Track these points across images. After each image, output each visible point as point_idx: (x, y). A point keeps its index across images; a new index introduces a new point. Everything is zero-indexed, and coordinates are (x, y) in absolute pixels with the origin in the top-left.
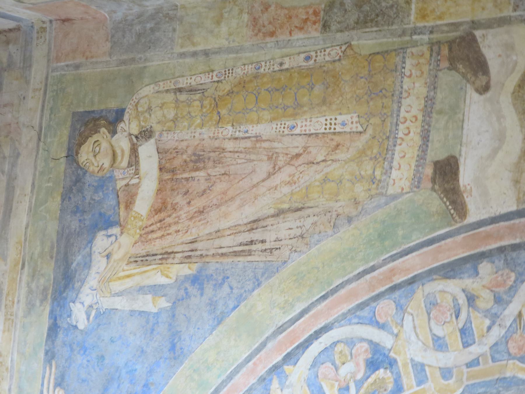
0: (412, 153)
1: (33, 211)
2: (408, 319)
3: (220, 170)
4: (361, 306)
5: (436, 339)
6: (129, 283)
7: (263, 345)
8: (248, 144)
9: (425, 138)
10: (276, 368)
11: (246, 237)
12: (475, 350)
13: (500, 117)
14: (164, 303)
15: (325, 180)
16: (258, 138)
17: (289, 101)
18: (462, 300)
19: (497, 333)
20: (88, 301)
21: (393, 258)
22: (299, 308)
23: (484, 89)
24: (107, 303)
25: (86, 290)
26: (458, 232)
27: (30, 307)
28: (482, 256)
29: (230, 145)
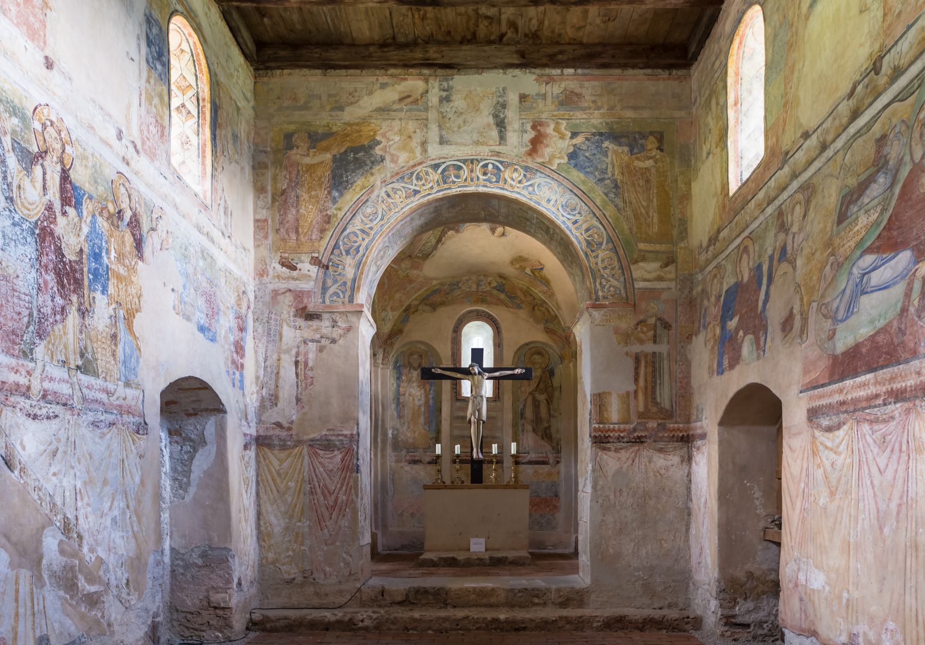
0: (647, 249)
2: (608, 252)
5: (604, 260)
6: (615, 161)
7: (600, 210)
9: (651, 252)
10: (595, 215)
14: (610, 175)
16: (652, 201)
19: (606, 276)
20: (610, 147)
22: (610, 220)
23: (661, 267)
24: (610, 154)
27: (607, 123)
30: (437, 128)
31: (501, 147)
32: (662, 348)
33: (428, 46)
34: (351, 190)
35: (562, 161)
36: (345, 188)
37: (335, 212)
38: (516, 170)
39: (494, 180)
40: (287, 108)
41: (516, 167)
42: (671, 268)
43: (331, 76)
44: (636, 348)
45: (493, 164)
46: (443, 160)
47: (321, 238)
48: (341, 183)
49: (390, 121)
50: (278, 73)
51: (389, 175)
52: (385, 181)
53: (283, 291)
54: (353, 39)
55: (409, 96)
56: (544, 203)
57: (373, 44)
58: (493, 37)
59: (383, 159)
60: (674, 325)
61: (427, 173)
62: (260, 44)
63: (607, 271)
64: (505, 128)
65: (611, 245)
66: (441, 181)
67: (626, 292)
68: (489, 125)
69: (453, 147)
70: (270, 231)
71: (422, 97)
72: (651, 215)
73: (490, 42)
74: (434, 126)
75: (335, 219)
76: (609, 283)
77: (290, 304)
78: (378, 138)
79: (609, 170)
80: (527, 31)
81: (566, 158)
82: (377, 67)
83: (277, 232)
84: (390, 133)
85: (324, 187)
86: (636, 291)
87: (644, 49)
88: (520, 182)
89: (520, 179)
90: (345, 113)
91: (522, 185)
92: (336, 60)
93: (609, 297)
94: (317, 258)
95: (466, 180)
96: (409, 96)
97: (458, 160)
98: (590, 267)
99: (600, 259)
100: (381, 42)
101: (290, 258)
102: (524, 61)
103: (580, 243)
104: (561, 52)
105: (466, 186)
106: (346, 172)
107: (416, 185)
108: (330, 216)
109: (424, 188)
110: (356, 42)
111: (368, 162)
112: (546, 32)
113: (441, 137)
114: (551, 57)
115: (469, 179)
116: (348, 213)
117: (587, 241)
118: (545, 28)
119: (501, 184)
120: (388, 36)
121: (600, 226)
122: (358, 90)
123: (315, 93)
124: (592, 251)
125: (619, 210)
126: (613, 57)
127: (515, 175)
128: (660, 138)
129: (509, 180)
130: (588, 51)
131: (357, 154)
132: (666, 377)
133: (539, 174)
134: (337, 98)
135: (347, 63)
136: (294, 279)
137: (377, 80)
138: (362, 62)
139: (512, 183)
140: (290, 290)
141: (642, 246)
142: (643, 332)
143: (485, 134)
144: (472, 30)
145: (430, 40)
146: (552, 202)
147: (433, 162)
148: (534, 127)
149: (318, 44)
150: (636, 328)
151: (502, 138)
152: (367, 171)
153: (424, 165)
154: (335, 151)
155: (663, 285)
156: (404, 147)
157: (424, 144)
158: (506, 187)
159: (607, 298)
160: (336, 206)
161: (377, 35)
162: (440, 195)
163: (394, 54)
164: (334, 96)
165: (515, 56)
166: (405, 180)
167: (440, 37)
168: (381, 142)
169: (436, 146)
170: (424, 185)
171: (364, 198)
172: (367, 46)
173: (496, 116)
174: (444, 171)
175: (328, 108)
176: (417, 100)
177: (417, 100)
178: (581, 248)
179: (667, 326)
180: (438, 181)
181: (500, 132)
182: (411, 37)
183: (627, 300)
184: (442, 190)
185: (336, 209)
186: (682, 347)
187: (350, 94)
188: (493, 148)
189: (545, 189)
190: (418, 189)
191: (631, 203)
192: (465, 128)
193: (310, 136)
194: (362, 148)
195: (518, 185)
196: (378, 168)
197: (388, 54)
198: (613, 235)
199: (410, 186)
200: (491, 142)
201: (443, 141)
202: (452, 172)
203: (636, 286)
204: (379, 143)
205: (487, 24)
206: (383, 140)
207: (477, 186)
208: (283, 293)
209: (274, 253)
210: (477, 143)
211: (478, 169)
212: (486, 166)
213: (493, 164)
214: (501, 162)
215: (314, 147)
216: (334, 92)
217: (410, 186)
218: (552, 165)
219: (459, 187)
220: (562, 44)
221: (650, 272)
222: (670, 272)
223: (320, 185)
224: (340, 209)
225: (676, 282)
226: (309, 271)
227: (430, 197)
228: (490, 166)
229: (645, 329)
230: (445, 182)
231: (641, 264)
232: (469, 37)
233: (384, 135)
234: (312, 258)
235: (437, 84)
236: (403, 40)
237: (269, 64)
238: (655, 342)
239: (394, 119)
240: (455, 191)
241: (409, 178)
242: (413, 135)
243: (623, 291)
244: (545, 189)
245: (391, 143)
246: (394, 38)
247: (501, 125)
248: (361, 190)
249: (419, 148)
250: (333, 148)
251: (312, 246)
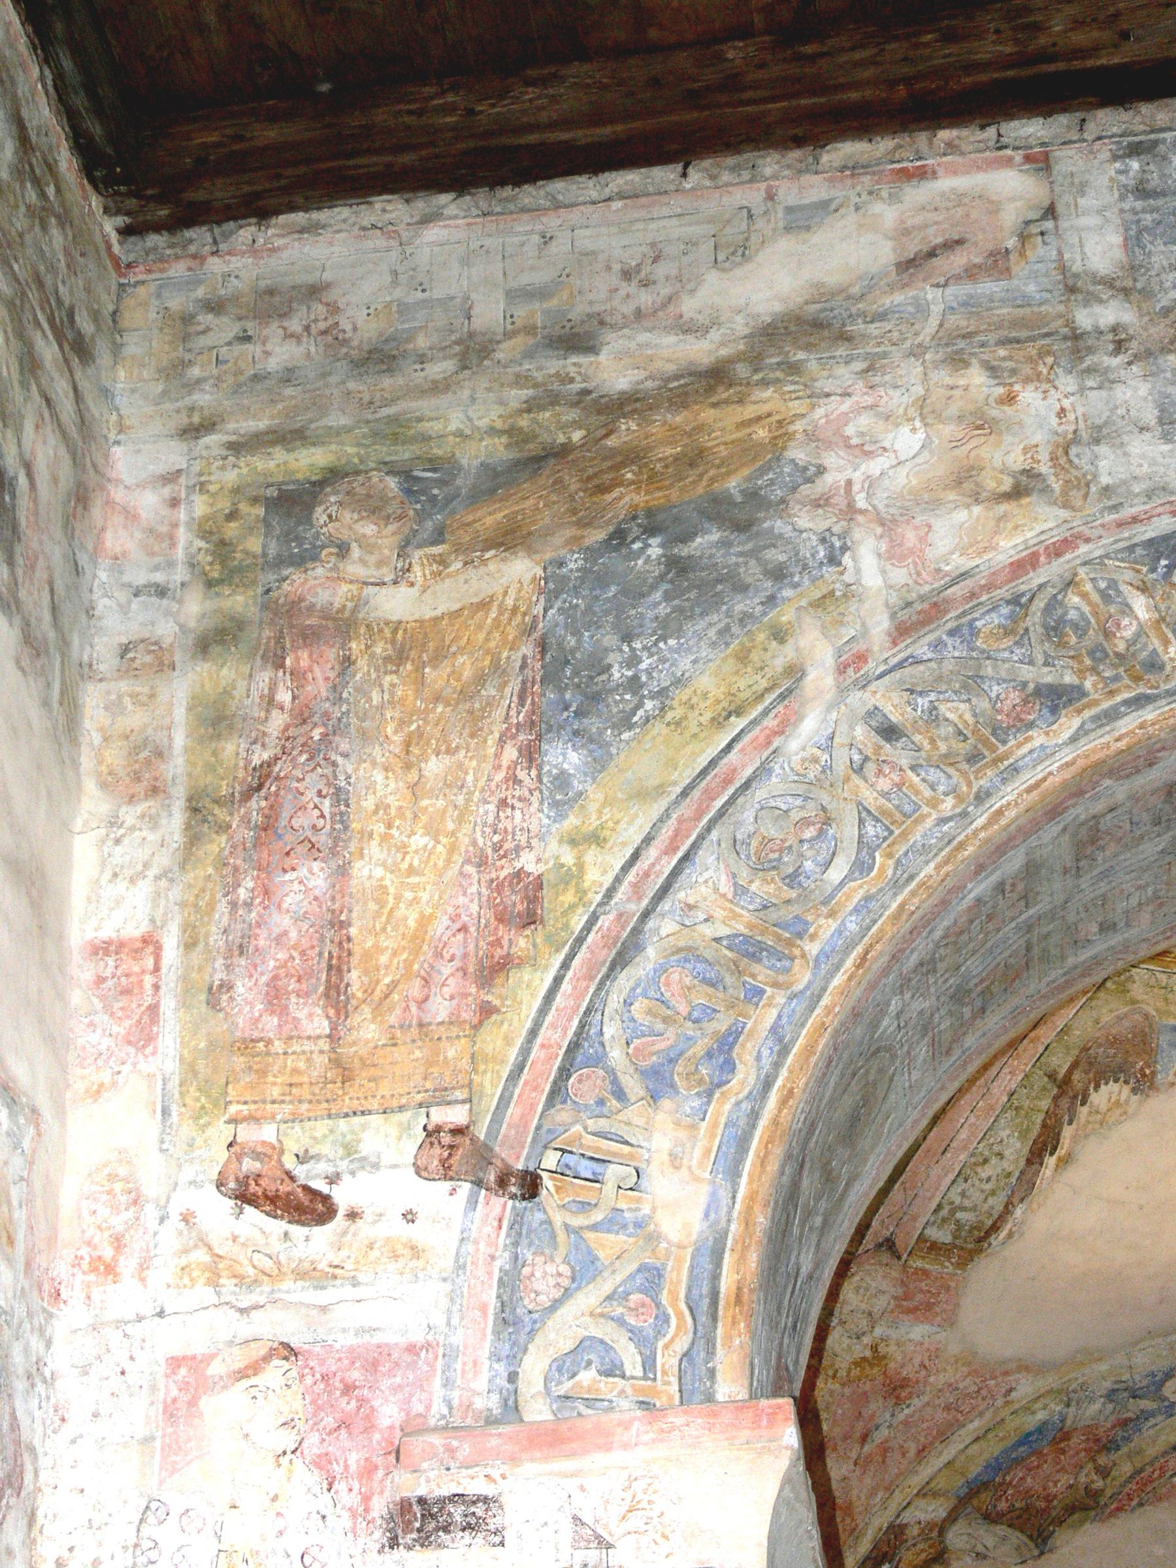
34: (658, 728)
36: (625, 722)
37: (568, 858)
43: (524, 210)
47: (487, 1011)
48: (594, 699)
52: (861, 658)
53: (238, 1359)
70: (168, 1004)
75: (569, 898)
77: (288, 1440)
83: (213, 1003)
85: (498, 729)
90: (603, 358)
92: (551, 126)
94: (458, 1131)
101: (292, 1145)
106: (627, 638)
108: (539, 883)
111: (752, 572)
116: (652, 852)
123: (438, 293)
131: (686, 538)
136: (309, 1274)
140: (288, 1351)
160: (572, 821)
171: (743, 763)
185: (573, 842)
208: (242, 1374)
209: (187, 1130)
223: (475, 725)
224: (596, 839)
226: (409, 1217)
227: (1149, 714)
234: (432, 1133)
248: (719, 722)
251: (429, 1063)
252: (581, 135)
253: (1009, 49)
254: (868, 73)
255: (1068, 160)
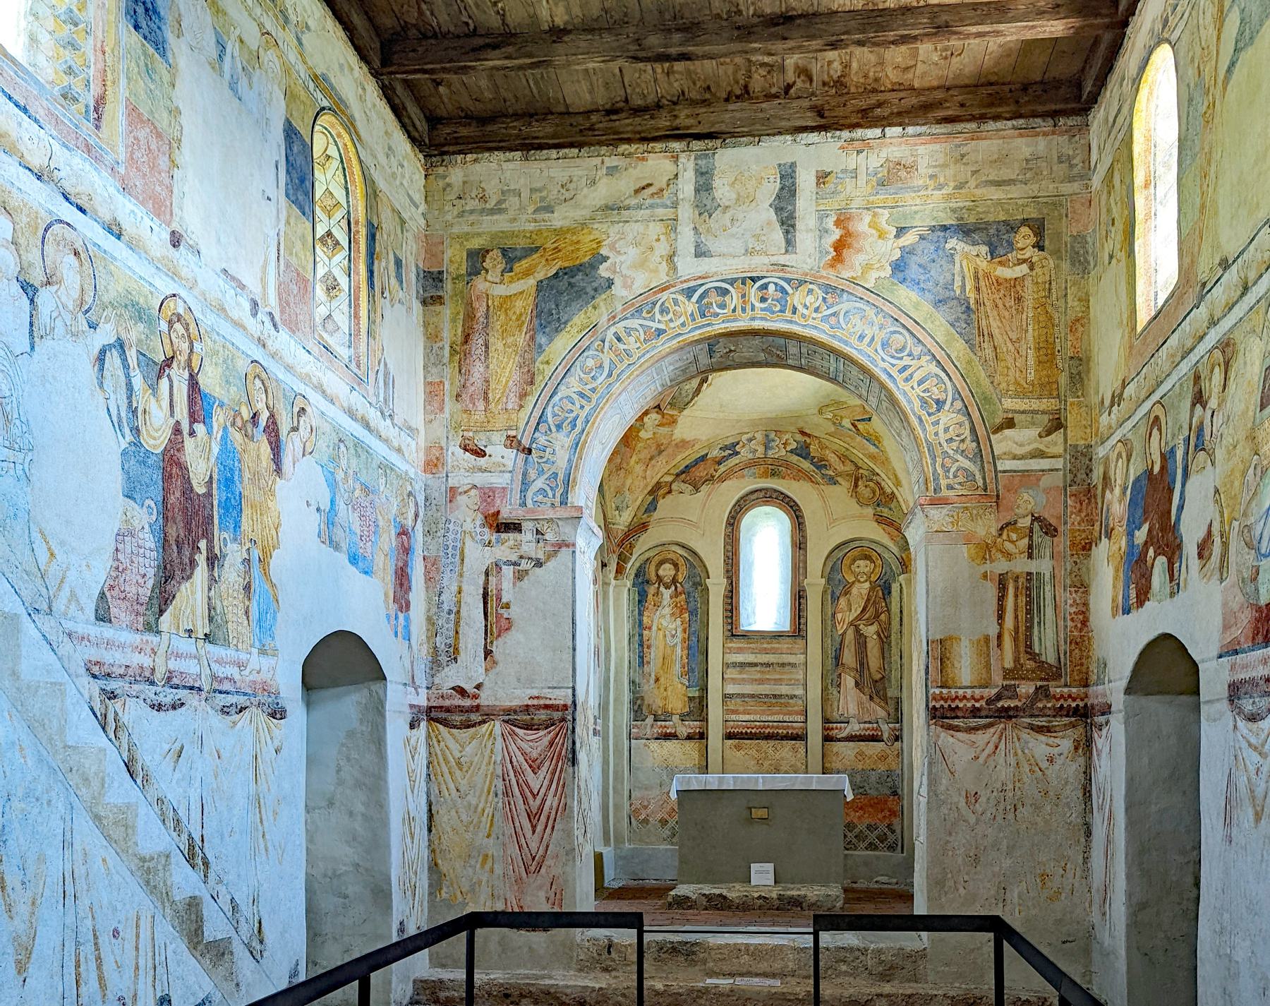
1: (999, 203)
3: (1014, 312)
4: (959, 393)
5: (948, 428)
7: (943, 349)
8: (1024, 326)
9: (1023, 412)
11: (986, 333)
12: (945, 445)
13: (1029, 444)
14: (958, 292)
15: (1008, 368)
17: (1041, 345)
18: (963, 437)
19: (951, 452)
21: (977, 405)
24: (957, 259)
25: (963, 245)
26: (987, 432)
28: (979, 443)
29: (1024, 316)
30: (692, 232)
31: (787, 256)
32: (1043, 566)
33: (677, 107)
35: (883, 275)
38: (810, 291)
39: (778, 308)
40: (472, 212)
41: (811, 286)
42: (1057, 436)
43: (536, 160)
44: (1001, 566)
45: (776, 284)
46: (700, 282)
49: (621, 224)
50: (459, 162)
51: (620, 308)
52: (614, 317)
54: (567, 106)
55: (650, 185)
56: (854, 341)
57: (597, 111)
58: (774, 90)
59: (610, 283)
60: (1061, 529)
61: (676, 302)
62: (433, 120)
63: (954, 445)
64: (793, 226)
65: (959, 404)
66: (697, 315)
67: (984, 479)
68: (769, 223)
69: (715, 260)
71: (668, 185)
72: (1024, 353)
73: (770, 97)
74: (687, 229)
76: (957, 464)
78: (604, 252)
79: (956, 285)
80: (826, 78)
81: (889, 270)
82: (600, 143)
84: (621, 242)
86: (999, 475)
87: (1011, 91)
88: (817, 310)
89: (817, 305)
91: (820, 315)
92: (542, 138)
93: (957, 486)
95: (734, 311)
96: (650, 185)
97: (722, 281)
98: (927, 440)
99: (941, 427)
100: (608, 107)
102: (823, 121)
103: (909, 402)
104: (880, 105)
105: (734, 321)
107: (659, 322)
109: (672, 325)
110: (571, 110)
111: (589, 290)
112: (855, 78)
113: (697, 246)
114: (864, 112)
115: (739, 309)
117: (922, 399)
118: (853, 72)
119: (788, 314)
120: (619, 99)
121: (943, 375)
122: (575, 179)
123: (512, 187)
124: (930, 415)
125: (972, 347)
126: (962, 105)
127: (810, 299)
128: (1038, 228)
129: (800, 307)
130: (923, 98)
132: (1049, 612)
133: (845, 295)
134: (544, 194)
135: (556, 141)
137: (603, 163)
138: (579, 139)
139: (805, 311)
141: (1008, 403)
142: (1013, 542)
143: (763, 238)
144: (742, 82)
145: (680, 99)
146: (867, 340)
147: (685, 286)
148: (838, 223)
149: (517, 116)
150: (1000, 535)
151: (790, 244)
152: (588, 303)
153: (672, 290)
154: (544, 272)
155: (1045, 464)
156: (641, 264)
157: (671, 258)
158: (796, 318)
159: (952, 488)
161: (602, 99)
162: (697, 334)
163: (626, 123)
164: (540, 190)
165: (809, 114)
166: (644, 314)
167: (694, 95)
168: (608, 258)
169: (690, 259)
170: (671, 320)
172: (588, 113)
173: (779, 210)
174: (702, 297)
175: (531, 209)
176: (662, 190)
177: (662, 190)
178: (913, 410)
179: (1050, 531)
180: (692, 315)
181: (787, 232)
182: (651, 99)
183: (985, 490)
184: (700, 328)
186: (1076, 563)
187: (562, 186)
188: (774, 259)
189: (856, 320)
190: (662, 326)
191: (991, 336)
192: (734, 230)
193: (504, 252)
194: (579, 268)
195: (815, 315)
196: (604, 296)
197: (617, 123)
198: (963, 387)
199: (651, 324)
200: (773, 250)
201: (700, 253)
202: (714, 298)
203: (999, 468)
204: (605, 259)
205: (765, 73)
206: (611, 255)
207: (753, 319)
210: (749, 252)
211: (753, 292)
212: (765, 287)
213: (776, 284)
214: (788, 281)
215: (511, 270)
216: (538, 185)
217: (651, 324)
218: (866, 281)
219: (723, 322)
220: (881, 92)
221: (1021, 445)
222: (1056, 444)
225: (1065, 459)
228: (772, 288)
229: (1014, 536)
230: (703, 315)
231: (1007, 432)
232: (738, 92)
233: (612, 247)
235: (691, 165)
236: (640, 102)
237: (446, 149)
238: (1030, 556)
239: (628, 222)
240: (719, 327)
241: (648, 312)
242: (655, 244)
243: (978, 477)
244: (856, 320)
245: (623, 258)
246: (626, 101)
247: (788, 223)
249: (664, 263)
250: (538, 270)
252: (551, 142)
253: (668, 124)
254: (630, 128)
255: (683, 158)
